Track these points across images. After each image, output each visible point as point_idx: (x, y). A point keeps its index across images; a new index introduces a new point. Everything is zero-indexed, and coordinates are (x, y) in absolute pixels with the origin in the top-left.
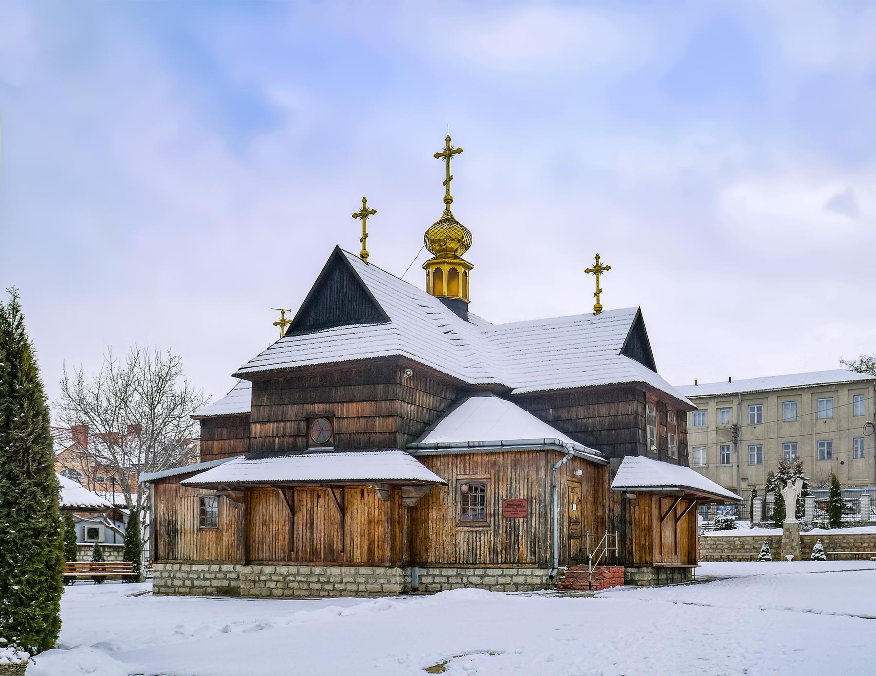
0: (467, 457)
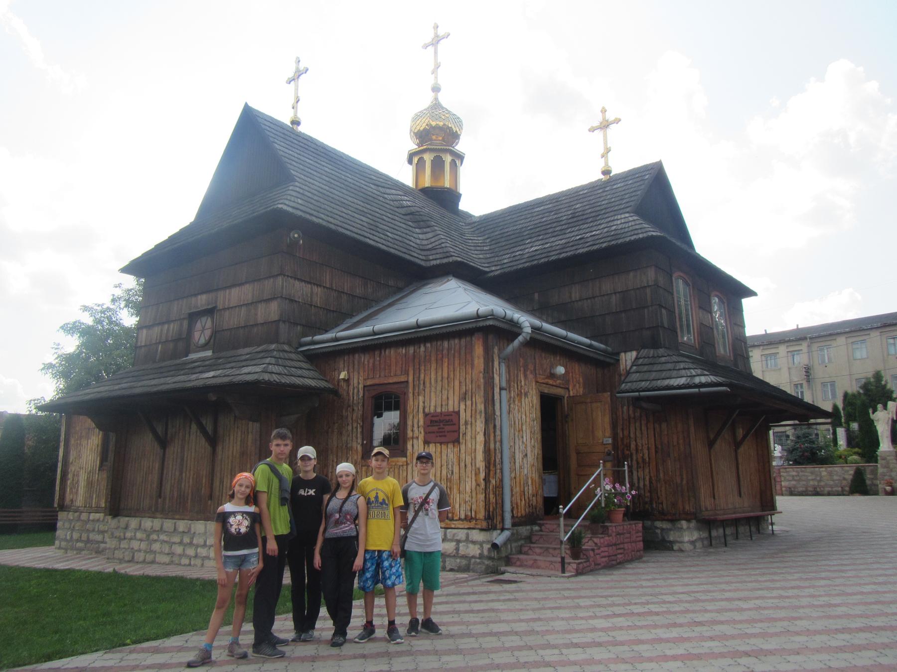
0: (377, 353)
